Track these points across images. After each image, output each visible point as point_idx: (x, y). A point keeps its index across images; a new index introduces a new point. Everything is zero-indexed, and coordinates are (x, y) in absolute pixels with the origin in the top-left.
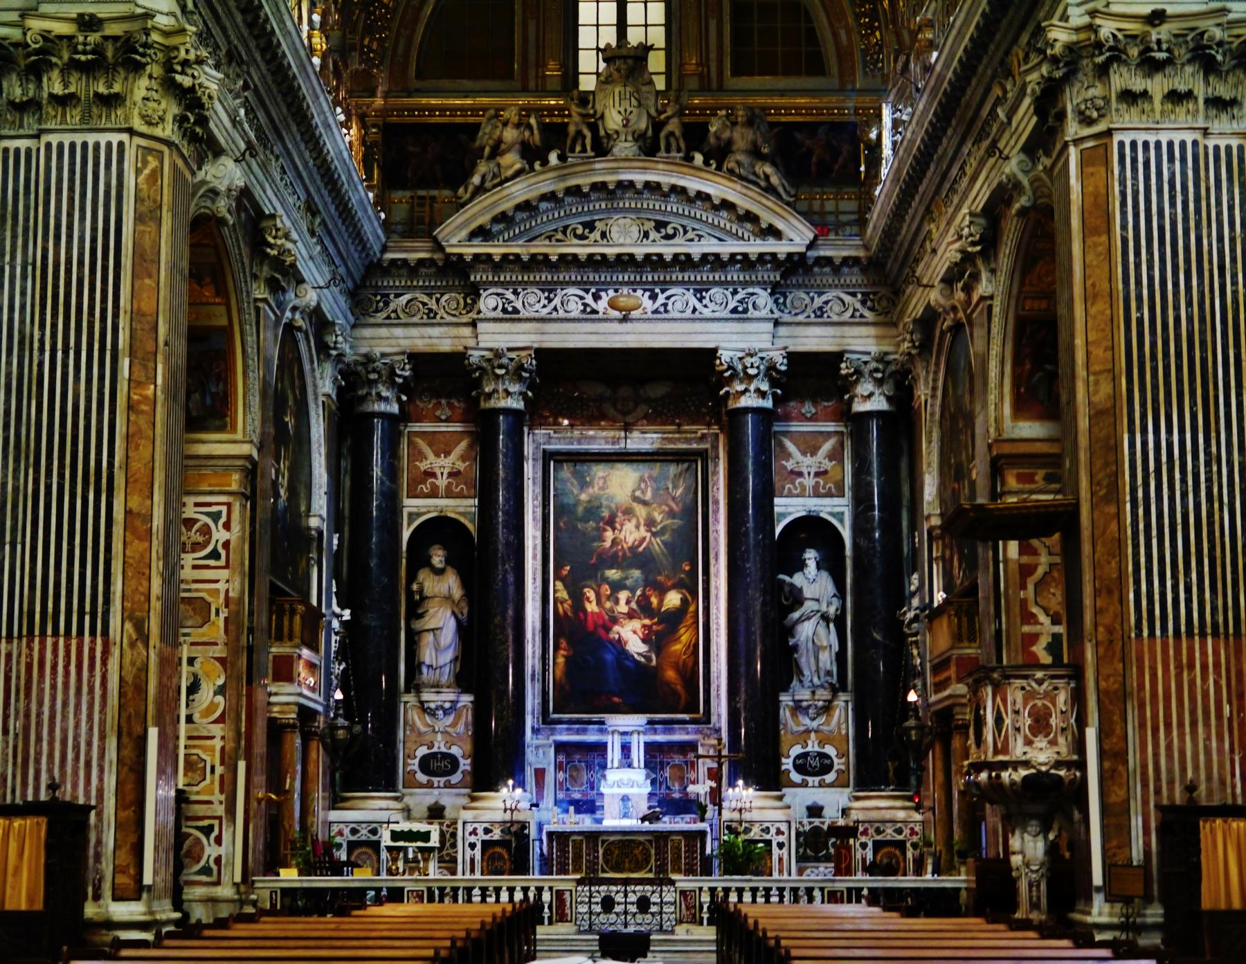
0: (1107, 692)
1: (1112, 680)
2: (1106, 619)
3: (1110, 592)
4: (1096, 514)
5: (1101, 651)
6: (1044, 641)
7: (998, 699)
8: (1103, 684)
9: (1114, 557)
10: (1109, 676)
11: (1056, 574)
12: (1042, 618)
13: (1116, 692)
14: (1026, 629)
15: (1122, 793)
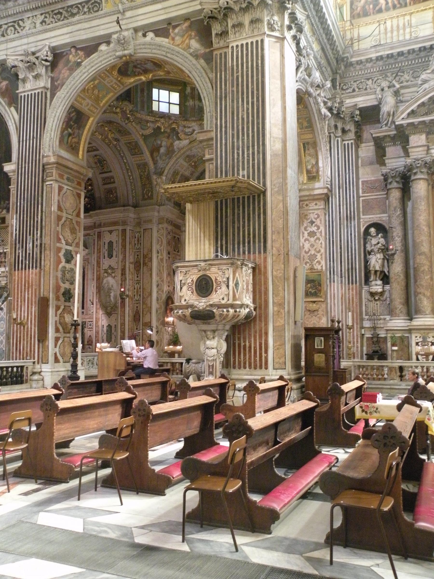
0: (276, 277)
1: (279, 271)
2: (277, 245)
3: (278, 233)
4: (273, 198)
5: (274, 258)
6: (63, 252)
7: (237, 275)
8: (275, 273)
9: (281, 219)
10: (277, 270)
11: (67, 222)
12: (63, 242)
13: (280, 277)
14: (58, 245)
15: (282, 322)
